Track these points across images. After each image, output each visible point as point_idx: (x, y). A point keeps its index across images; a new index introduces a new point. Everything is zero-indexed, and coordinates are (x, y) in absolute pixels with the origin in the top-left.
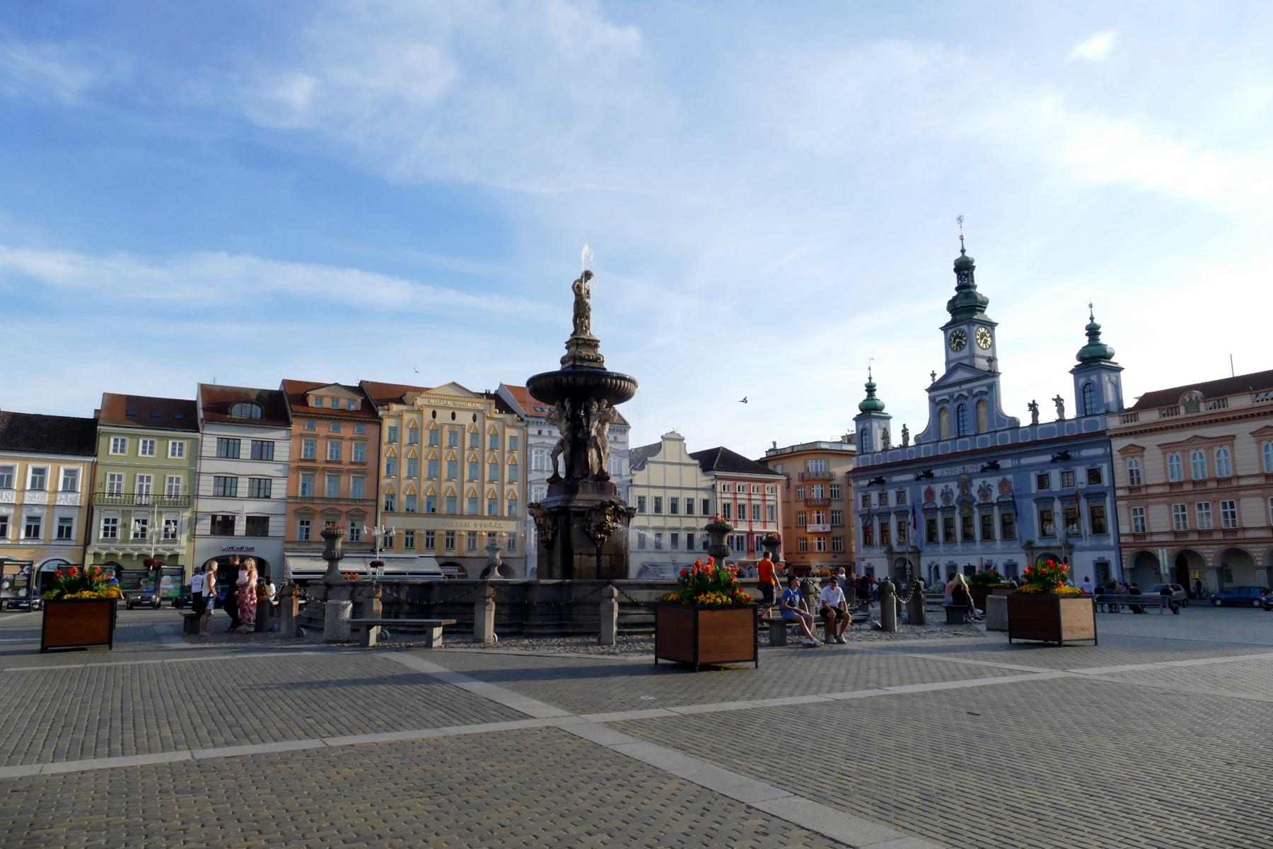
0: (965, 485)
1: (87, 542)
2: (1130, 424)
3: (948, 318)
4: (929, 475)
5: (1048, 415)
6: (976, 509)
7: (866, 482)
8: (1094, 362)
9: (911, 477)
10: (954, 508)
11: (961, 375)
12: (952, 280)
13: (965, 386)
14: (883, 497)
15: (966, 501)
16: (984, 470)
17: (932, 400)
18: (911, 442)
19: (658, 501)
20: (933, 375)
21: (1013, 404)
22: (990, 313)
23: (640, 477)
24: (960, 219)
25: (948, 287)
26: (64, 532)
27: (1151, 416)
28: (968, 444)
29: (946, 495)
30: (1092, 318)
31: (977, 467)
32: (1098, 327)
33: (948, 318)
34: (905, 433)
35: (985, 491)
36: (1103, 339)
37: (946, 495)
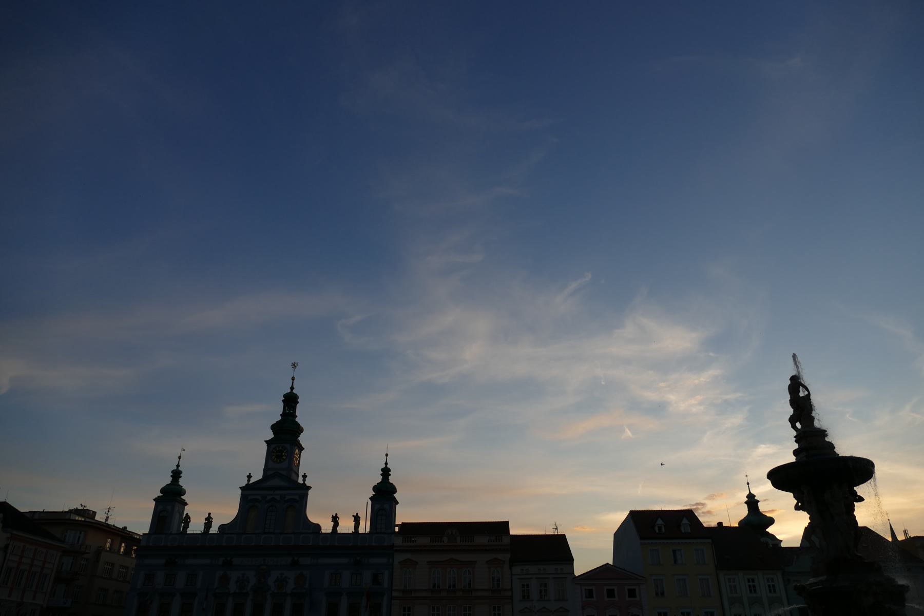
2: (409, 544)
3: (270, 435)
5: (346, 526)
8: (384, 495)
11: (276, 482)
12: (279, 408)
13: (278, 490)
17: (244, 498)
18: (214, 530)
20: (249, 477)
21: (318, 514)
22: (302, 439)
24: (294, 365)
25: (276, 411)
27: (424, 541)
30: (386, 464)
32: (389, 470)
33: (270, 435)
34: (209, 521)
36: (392, 479)
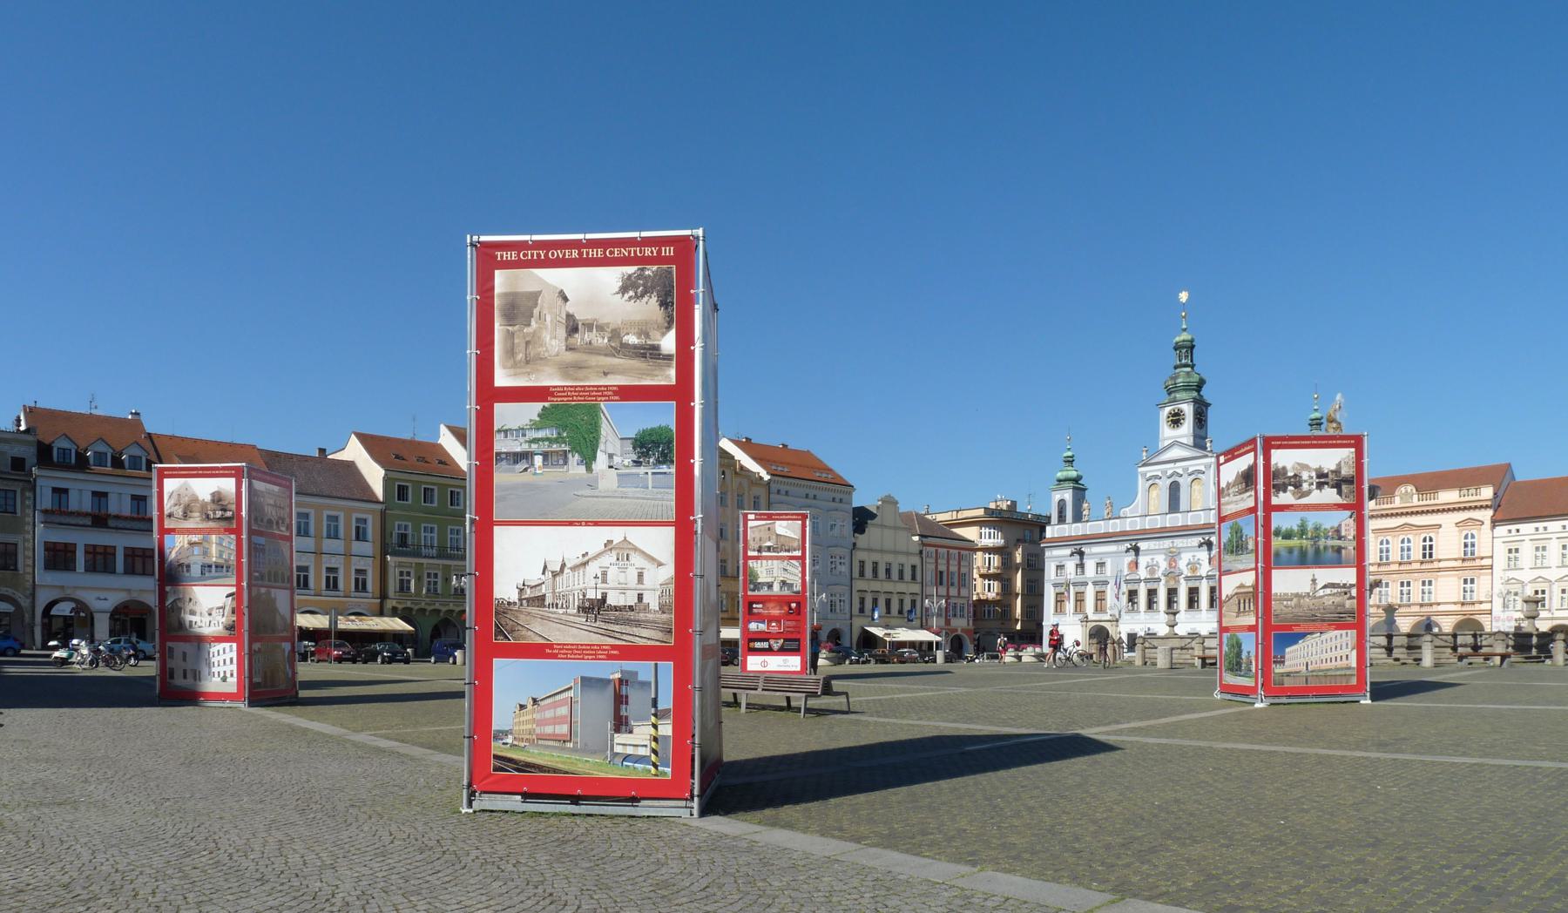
0: (1173, 557)
1: (384, 596)
4: (1137, 550)
6: (1182, 581)
7: (1068, 551)
9: (1112, 548)
10: (1159, 580)
14: (1081, 566)
15: (1172, 574)
16: (1201, 545)
19: (875, 565)
23: (862, 540)
26: (361, 586)
28: (1178, 520)
29: (1152, 568)
31: (1196, 541)
35: (1193, 566)
37: (1152, 568)
